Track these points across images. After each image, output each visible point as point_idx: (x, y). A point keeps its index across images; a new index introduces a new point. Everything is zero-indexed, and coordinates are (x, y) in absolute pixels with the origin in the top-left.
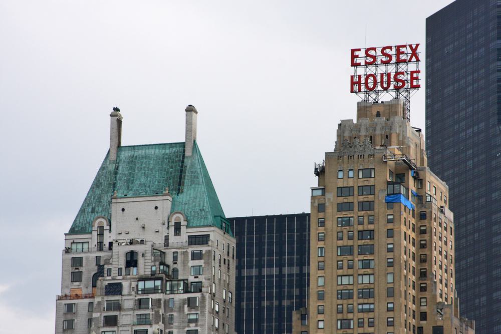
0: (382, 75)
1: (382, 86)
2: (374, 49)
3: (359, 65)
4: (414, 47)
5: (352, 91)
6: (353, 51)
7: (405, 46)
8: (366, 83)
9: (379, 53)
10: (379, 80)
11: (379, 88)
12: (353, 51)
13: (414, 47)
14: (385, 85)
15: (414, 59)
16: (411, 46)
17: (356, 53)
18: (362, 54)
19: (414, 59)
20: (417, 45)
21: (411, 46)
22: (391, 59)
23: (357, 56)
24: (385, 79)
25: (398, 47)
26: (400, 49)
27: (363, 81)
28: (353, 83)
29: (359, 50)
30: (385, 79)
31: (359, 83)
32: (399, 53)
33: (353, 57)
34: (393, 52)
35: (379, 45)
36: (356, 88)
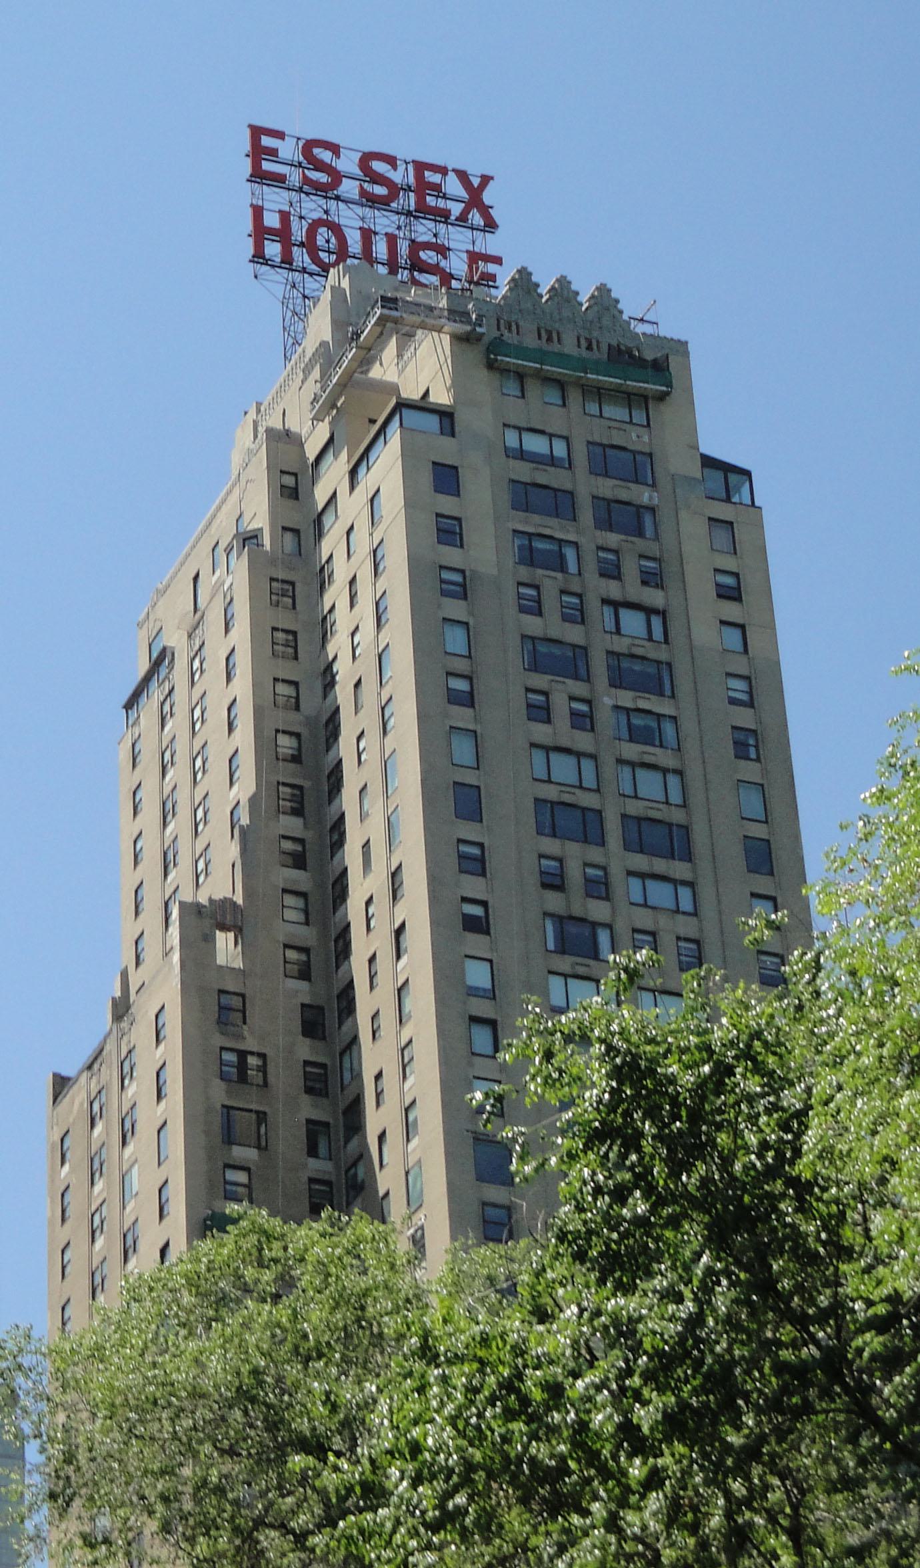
0: (367, 235)
2: (335, 149)
3: (278, 180)
4: (476, 182)
5: (259, 256)
6: (257, 132)
7: (443, 171)
8: (310, 245)
9: (348, 163)
12: (257, 132)
13: (476, 182)
15: (476, 218)
16: (463, 176)
18: (288, 150)
20: (486, 179)
21: (463, 176)
23: (273, 152)
24: (381, 249)
26: (427, 173)
27: (299, 232)
28: (260, 232)
29: (280, 135)
31: (283, 234)
32: (422, 187)
33: (258, 153)
35: (355, 137)
36: (273, 249)
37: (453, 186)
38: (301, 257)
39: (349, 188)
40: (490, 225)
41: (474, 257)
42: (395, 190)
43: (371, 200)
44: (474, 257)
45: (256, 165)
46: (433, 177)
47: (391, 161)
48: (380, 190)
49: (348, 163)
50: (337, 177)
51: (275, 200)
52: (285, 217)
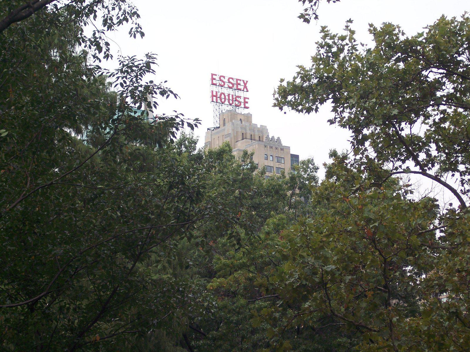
1: (229, 102)
2: (224, 77)
3: (216, 85)
4: (245, 82)
6: (212, 75)
7: (240, 80)
8: (220, 97)
9: (226, 80)
10: (227, 98)
11: (227, 102)
12: (212, 75)
14: (231, 102)
15: (245, 90)
16: (243, 81)
17: (214, 77)
18: (217, 78)
19: (245, 90)
20: (247, 82)
22: (233, 86)
23: (215, 79)
24: (231, 98)
25: (237, 80)
28: (213, 96)
29: (216, 75)
30: (231, 98)
31: (216, 96)
33: (213, 79)
34: (234, 82)
35: (227, 76)
36: (215, 98)
37: (242, 83)
38: (219, 100)
39: (226, 86)
40: (247, 91)
41: (245, 98)
42: (233, 84)
43: (230, 88)
44: (245, 98)
45: (212, 81)
46: (239, 82)
47: (233, 79)
48: (231, 85)
49: (226, 80)
50: (224, 82)
51: (215, 89)
52: (217, 92)
